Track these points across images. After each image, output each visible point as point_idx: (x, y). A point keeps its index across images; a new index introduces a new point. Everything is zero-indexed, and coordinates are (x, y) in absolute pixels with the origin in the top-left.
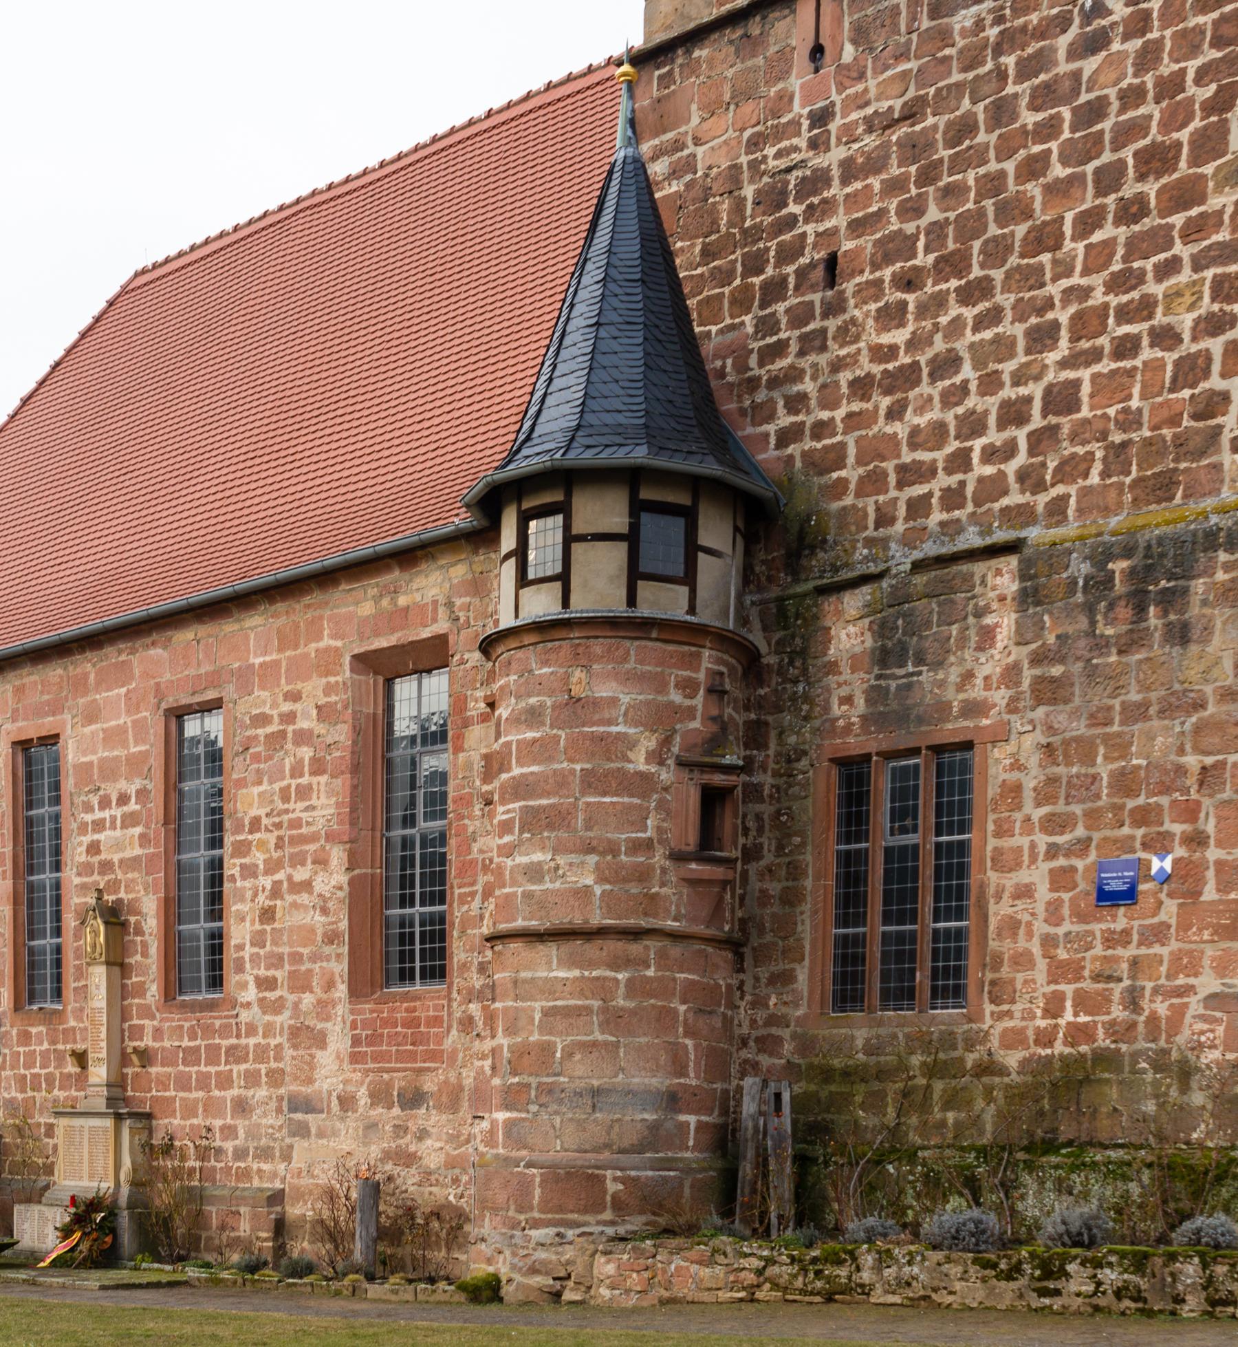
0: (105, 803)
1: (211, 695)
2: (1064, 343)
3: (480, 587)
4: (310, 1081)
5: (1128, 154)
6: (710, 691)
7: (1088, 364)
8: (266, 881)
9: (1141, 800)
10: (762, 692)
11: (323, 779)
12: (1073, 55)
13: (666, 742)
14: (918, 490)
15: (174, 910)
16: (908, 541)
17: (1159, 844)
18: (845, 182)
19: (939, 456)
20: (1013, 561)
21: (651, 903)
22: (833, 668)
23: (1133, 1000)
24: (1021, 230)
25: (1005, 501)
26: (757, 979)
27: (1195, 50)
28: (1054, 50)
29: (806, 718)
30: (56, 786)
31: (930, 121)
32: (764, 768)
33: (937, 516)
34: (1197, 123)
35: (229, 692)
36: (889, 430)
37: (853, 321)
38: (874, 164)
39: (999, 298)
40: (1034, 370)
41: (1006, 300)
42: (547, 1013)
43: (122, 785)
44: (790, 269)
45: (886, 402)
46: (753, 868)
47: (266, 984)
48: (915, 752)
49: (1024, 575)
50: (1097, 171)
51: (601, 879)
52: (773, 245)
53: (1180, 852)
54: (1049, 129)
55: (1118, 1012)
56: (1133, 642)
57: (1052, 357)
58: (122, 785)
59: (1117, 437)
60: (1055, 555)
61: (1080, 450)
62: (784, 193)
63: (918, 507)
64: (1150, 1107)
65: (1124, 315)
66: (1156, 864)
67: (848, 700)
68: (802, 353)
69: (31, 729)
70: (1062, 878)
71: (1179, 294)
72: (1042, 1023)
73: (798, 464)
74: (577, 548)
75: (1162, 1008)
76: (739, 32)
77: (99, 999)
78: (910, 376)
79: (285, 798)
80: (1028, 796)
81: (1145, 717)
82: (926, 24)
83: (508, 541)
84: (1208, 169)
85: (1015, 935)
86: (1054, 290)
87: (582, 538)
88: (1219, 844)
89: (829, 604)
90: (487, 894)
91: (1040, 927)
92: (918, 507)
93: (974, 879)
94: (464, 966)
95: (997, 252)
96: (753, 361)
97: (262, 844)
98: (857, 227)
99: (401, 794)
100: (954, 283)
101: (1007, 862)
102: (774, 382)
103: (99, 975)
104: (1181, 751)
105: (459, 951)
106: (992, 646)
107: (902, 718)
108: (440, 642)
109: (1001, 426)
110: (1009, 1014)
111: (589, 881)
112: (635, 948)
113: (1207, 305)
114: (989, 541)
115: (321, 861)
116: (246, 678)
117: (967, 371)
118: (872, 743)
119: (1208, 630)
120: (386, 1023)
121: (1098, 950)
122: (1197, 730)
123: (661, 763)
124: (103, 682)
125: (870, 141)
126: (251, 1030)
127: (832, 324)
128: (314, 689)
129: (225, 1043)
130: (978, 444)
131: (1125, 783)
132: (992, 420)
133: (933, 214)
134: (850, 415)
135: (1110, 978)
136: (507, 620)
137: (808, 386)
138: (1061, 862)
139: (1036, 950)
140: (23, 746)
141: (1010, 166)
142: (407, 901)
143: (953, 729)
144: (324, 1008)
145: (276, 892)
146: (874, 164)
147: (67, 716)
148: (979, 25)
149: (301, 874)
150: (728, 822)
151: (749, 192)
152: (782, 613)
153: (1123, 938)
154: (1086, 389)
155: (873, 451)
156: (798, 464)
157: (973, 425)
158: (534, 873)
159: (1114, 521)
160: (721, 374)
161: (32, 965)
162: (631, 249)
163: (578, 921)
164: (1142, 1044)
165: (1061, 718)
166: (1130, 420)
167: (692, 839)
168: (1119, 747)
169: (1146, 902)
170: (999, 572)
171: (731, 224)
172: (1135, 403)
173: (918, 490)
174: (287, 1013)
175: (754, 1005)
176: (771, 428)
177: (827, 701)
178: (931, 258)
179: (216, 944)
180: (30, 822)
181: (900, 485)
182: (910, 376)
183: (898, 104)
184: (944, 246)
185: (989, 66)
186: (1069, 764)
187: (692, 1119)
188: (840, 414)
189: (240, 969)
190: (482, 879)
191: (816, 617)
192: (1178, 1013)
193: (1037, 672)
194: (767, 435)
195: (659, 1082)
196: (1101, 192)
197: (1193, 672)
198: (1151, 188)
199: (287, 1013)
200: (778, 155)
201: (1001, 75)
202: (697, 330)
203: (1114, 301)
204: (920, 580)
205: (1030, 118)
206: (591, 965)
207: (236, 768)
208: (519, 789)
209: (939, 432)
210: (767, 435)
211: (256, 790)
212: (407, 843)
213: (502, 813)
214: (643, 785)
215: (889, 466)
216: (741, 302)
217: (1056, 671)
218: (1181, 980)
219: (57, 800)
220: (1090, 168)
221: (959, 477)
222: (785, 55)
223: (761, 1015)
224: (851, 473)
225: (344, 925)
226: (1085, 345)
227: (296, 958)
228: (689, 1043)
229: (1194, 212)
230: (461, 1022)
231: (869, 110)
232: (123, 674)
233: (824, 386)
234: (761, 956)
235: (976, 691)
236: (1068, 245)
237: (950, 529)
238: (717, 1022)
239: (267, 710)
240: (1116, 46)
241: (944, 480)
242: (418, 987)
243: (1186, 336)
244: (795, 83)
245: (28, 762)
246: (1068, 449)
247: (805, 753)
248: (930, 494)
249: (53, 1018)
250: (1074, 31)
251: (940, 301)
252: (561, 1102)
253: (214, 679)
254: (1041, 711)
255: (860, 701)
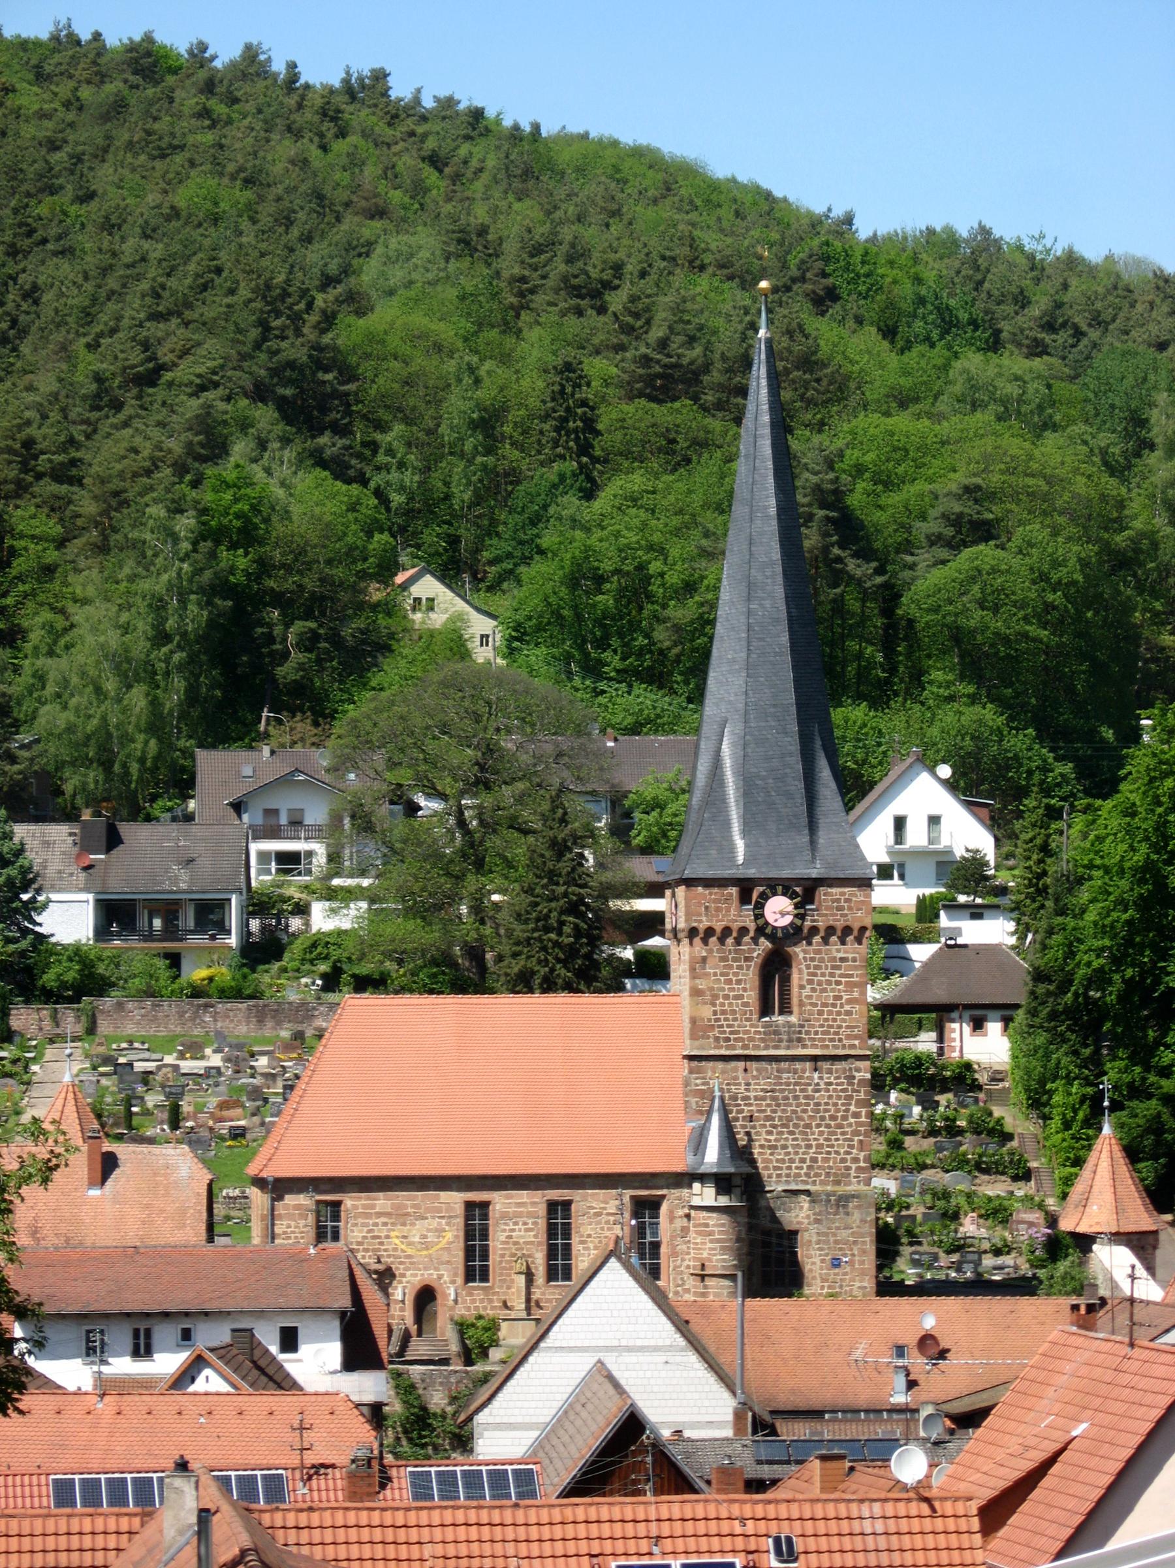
17: (845, 1255)
38: (763, 1099)
70: (823, 1261)
168: (835, 1235)
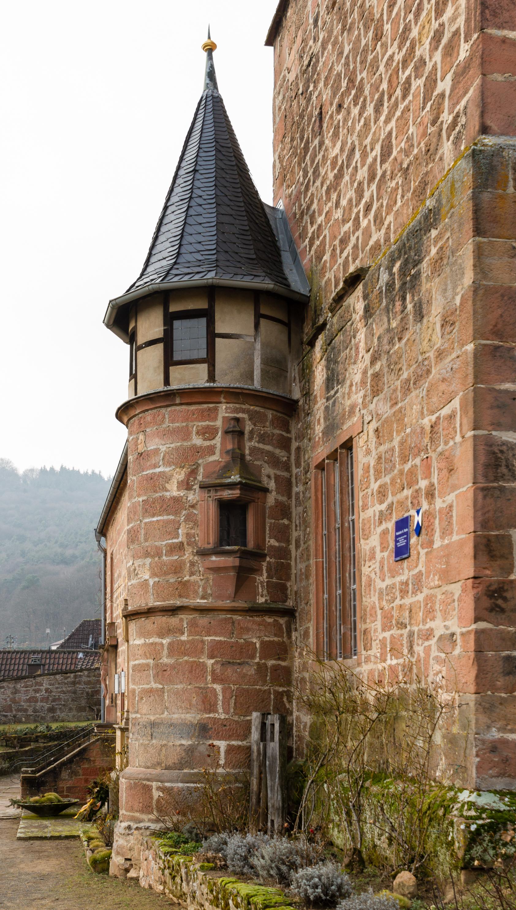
13: (193, 472)
112: (174, 621)
123: (189, 488)
187: (222, 745)
228: (218, 687)
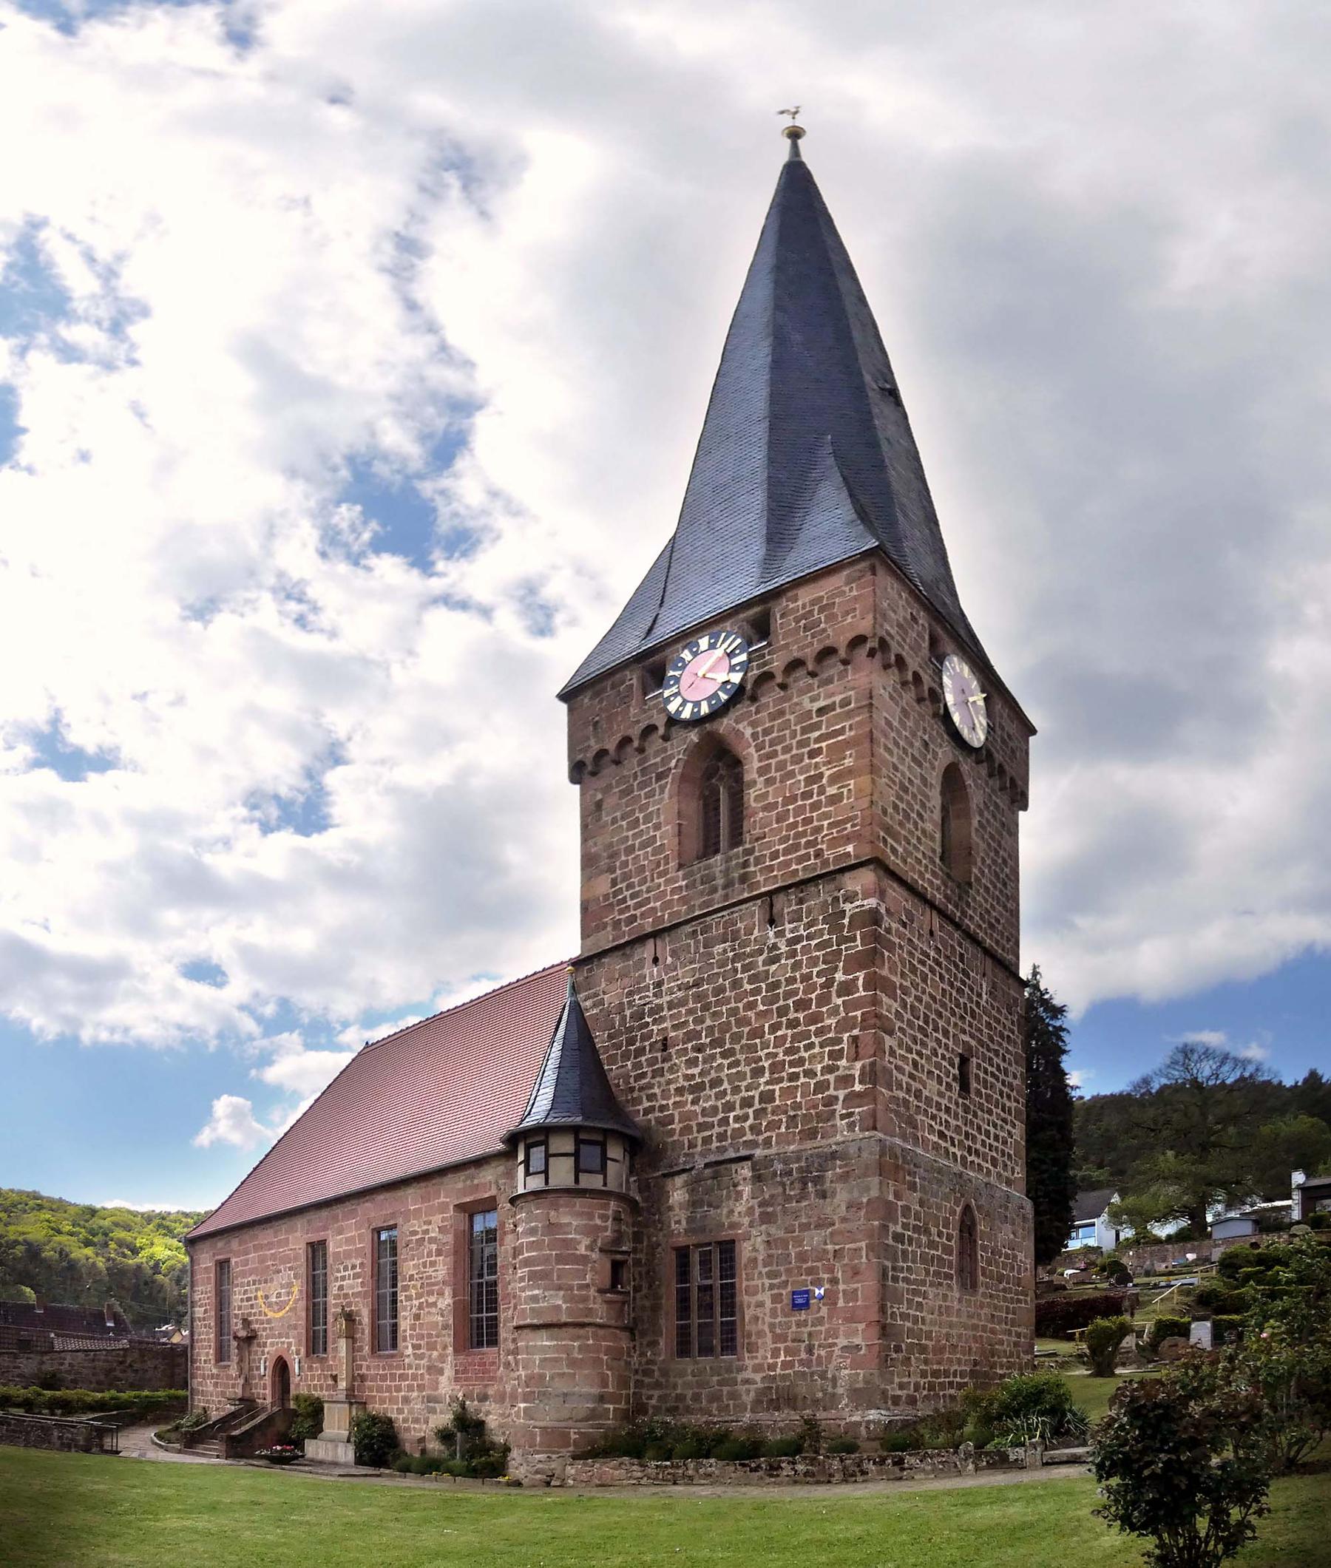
0: (346, 1269)
1: (392, 1222)
2: (767, 1075)
3: (511, 1175)
4: (437, 1389)
5: (790, 1002)
6: (614, 1219)
7: (777, 1084)
8: (416, 1302)
9: (809, 1264)
10: (640, 1219)
11: (441, 1258)
12: (764, 964)
13: (595, 1241)
14: (708, 1133)
15: (376, 1314)
16: (703, 1155)
17: (818, 1283)
18: (670, 1009)
19: (715, 1120)
20: (749, 1163)
21: (590, 1312)
22: (670, 1208)
23: (810, 1350)
24: (746, 1030)
25: (745, 1139)
26: (641, 1344)
27: (815, 965)
28: (757, 962)
29: (661, 1230)
30: (325, 1262)
31: (706, 987)
32: (642, 1251)
33: (715, 1145)
34: (818, 992)
35: (400, 1221)
36: (693, 1108)
37: (675, 1064)
39: (738, 1056)
40: (755, 1085)
41: (741, 1057)
42: (542, 1361)
43: (354, 1261)
44: (647, 1043)
45: (690, 1097)
46: (638, 1295)
47: (416, 1347)
48: (709, 1244)
49: (753, 1169)
50: (777, 1008)
51: (564, 1302)
52: (639, 1034)
53: (827, 1286)
54: (756, 991)
55: (804, 1356)
56: (802, 1198)
57: (762, 1080)
58: (354, 1261)
59: (792, 1113)
60: (768, 1161)
61: (776, 1118)
62: (644, 1013)
63: (707, 1141)
64: (820, 1395)
65: (792, 1064)
66: (817, 1292)
67: (678, 1222)
68: (653, 1077)
69: (314, 1237)
70: (776, 1299)
71: (814, 1057)
72: (771, 1361)
73: (653, 1123)
74: (552, 1160)
75: (823, 1353)
76: (621, 953)
77: (343, 1353)
78: (701, 1087)
79: (425, 1267)
80: (760, 1263)
81: (809, 1229)
82: (702, 950)
83: (521, 1157)
84: (824, 1009)
85: (757, 1324)
86: (762, 1053)
87: (555, 1155)
88: (844, 1283)
89: (669, 1182)
90: (515, 1308)
91: (768, 1319)
92: (707, 1141)
93: (737, 1299)
94: (506, 1340)
95: (736, 1038)
96: (632, 1080)
97: (414, 1286)
98: (675, 1027)
99: (477, 1264)
100: (718, 1050)
101: (753, 1292)
102: (641, 1089)
103: (342, 1343)
104: (826, 1244)
105: (504, 1333)
106: (742, 1199)
107: (703, 1230)
108: (493, 1198)
109: (741, 1108)
110: (756, 1358)
111: (560, 1303)
112: (582, 1332)
113: (826, 1061)
114: (738, 1155)
115: (441, 1294)
116: (407, 1215)
117: (726, 1085)
118: (692, 1240)
119: (834, 1193)
120: (470, 1364)
121: (794, 1329)
122: (831, 1233)
123: (592, 1250)
124: (346, 1218)
125: (680, 994)
126: (410, 1367)
127: (666, 1066)
128: (437, 1219)
129: (398, 1372)
130: (732, 1115)
131: (802, 1257)
132: (738, 1106)
133: (708, 1022)
134: (675, 1103)
135: (799, 1341)
136: (521, 1191)
137: (656, 1090)
138: (775, 1291)
139: (767, 1329)
140: (311, 1245)
141: (740, 1005)
142: (480, 1311)
143: (725, 1235)
144: (442, 1358)
145: (420, 1307)
146: (682, 1002)
147: (330, 1232)
148: (725, 951)
149: (431, 1300)
150: (625, 1275)
151: (628, 1013)
152: (648, 1186)
153: (805, 1323)
154: (777, 1093)
155: (687, 1117)
156: (653, 1123)
157: (729, 1107)
158: (534, 1299)
159: (792, 1148)
160: (618, 1085)
161: (314, 1338)
162: (574, 1036)
163: (555, 1320)
164: (814, 1369)
165: (773, 1230)
166: (797, 1106)
167: (607, 1283)
168: (799, 1242)
169: (813, 1308)
170: (743, 1168)
171: (620, 1025)
172: (798, 1100)
173: (708, 1133)
174: (426, 1360)
175: (640, 1355)
176: (640, 1107)
177: (670, 1223)
178: (708, 1040)
179: (395, 1327)
180: (314, 1276)
181: (698, 1132)
182: (701, 1087)
183: (691, 980)
184: (714, 1035)
185: (730, 967)
186: (777, 1248)
187: (611, 1407)
188: (671, 1102)
189: (405, 1340)
190: (513, 1302)
191: (663, 1187)
192: (830, 1355)
193: (761, 1210)
194: (639, 1111)
195: (595, 1391)
196: (779, 1016)
197: (829, 1210)
198: (801, 1016)
199: (426, 1360)
200: (640, 999)
201: (736, 970)
202: (606, 1067)
203: (787, 1059)
204: (708, 1171)
205: (748, 987)
206: (562, 1340)
207: (403, 1253)
208: (527, 1262)
209: (714, 1110)
210: (639, 1111)
211: (412, 1263)
212: (480, 1285)
213: (520, 1273)
214: (584, 1260)
215: (693, 1123)
216: (626, 1056)
217: (770, 1209)
218: (830, 1341)
219: (325, 1268)
220: (775, 1007)
221: (724, 1128)
222: (642, 960)
223: (644, 1360)
224: (676, 1126)
225: (451, 1322)
226: (776, 1076)
227: (430, 1336)
228: (609, 1373)
229: (819, 1025)
230: (505, 1364)
231: (679, 982)
232: (353, 1214)
233: (663, 1091)
234: (643, 1334)
235: (735, 1218)
236: (767, 1036)
237: (721, 1150)
238: (622, 1363)
239: (416, 1228)
240: (783, 961)
241: (717, 1130)
242: (485, 1349)
243: (819, 1074)
244: (646, 971)
245: (314, 1252)
246: (770, 1117)
247: (659, 1245)
248: (712, 1135)
249: (323, 1361)
250: (765, 955)
251: (713, 1057)
252: (549, 1399)
253: (393, 1215)
254: (764, 1227)
255: (684, 1222)
